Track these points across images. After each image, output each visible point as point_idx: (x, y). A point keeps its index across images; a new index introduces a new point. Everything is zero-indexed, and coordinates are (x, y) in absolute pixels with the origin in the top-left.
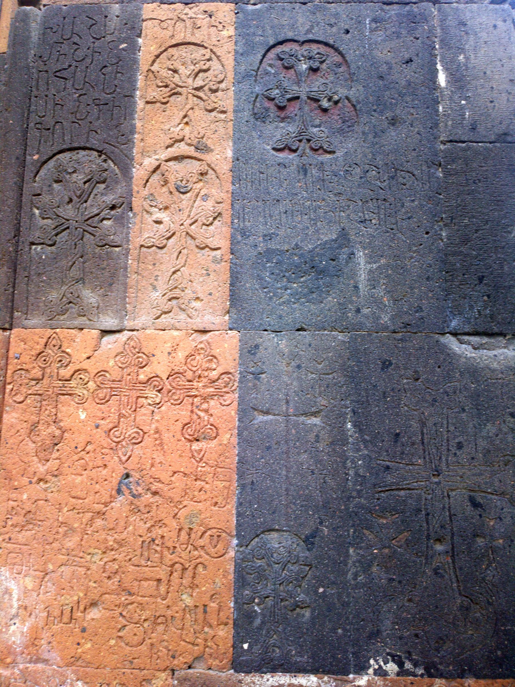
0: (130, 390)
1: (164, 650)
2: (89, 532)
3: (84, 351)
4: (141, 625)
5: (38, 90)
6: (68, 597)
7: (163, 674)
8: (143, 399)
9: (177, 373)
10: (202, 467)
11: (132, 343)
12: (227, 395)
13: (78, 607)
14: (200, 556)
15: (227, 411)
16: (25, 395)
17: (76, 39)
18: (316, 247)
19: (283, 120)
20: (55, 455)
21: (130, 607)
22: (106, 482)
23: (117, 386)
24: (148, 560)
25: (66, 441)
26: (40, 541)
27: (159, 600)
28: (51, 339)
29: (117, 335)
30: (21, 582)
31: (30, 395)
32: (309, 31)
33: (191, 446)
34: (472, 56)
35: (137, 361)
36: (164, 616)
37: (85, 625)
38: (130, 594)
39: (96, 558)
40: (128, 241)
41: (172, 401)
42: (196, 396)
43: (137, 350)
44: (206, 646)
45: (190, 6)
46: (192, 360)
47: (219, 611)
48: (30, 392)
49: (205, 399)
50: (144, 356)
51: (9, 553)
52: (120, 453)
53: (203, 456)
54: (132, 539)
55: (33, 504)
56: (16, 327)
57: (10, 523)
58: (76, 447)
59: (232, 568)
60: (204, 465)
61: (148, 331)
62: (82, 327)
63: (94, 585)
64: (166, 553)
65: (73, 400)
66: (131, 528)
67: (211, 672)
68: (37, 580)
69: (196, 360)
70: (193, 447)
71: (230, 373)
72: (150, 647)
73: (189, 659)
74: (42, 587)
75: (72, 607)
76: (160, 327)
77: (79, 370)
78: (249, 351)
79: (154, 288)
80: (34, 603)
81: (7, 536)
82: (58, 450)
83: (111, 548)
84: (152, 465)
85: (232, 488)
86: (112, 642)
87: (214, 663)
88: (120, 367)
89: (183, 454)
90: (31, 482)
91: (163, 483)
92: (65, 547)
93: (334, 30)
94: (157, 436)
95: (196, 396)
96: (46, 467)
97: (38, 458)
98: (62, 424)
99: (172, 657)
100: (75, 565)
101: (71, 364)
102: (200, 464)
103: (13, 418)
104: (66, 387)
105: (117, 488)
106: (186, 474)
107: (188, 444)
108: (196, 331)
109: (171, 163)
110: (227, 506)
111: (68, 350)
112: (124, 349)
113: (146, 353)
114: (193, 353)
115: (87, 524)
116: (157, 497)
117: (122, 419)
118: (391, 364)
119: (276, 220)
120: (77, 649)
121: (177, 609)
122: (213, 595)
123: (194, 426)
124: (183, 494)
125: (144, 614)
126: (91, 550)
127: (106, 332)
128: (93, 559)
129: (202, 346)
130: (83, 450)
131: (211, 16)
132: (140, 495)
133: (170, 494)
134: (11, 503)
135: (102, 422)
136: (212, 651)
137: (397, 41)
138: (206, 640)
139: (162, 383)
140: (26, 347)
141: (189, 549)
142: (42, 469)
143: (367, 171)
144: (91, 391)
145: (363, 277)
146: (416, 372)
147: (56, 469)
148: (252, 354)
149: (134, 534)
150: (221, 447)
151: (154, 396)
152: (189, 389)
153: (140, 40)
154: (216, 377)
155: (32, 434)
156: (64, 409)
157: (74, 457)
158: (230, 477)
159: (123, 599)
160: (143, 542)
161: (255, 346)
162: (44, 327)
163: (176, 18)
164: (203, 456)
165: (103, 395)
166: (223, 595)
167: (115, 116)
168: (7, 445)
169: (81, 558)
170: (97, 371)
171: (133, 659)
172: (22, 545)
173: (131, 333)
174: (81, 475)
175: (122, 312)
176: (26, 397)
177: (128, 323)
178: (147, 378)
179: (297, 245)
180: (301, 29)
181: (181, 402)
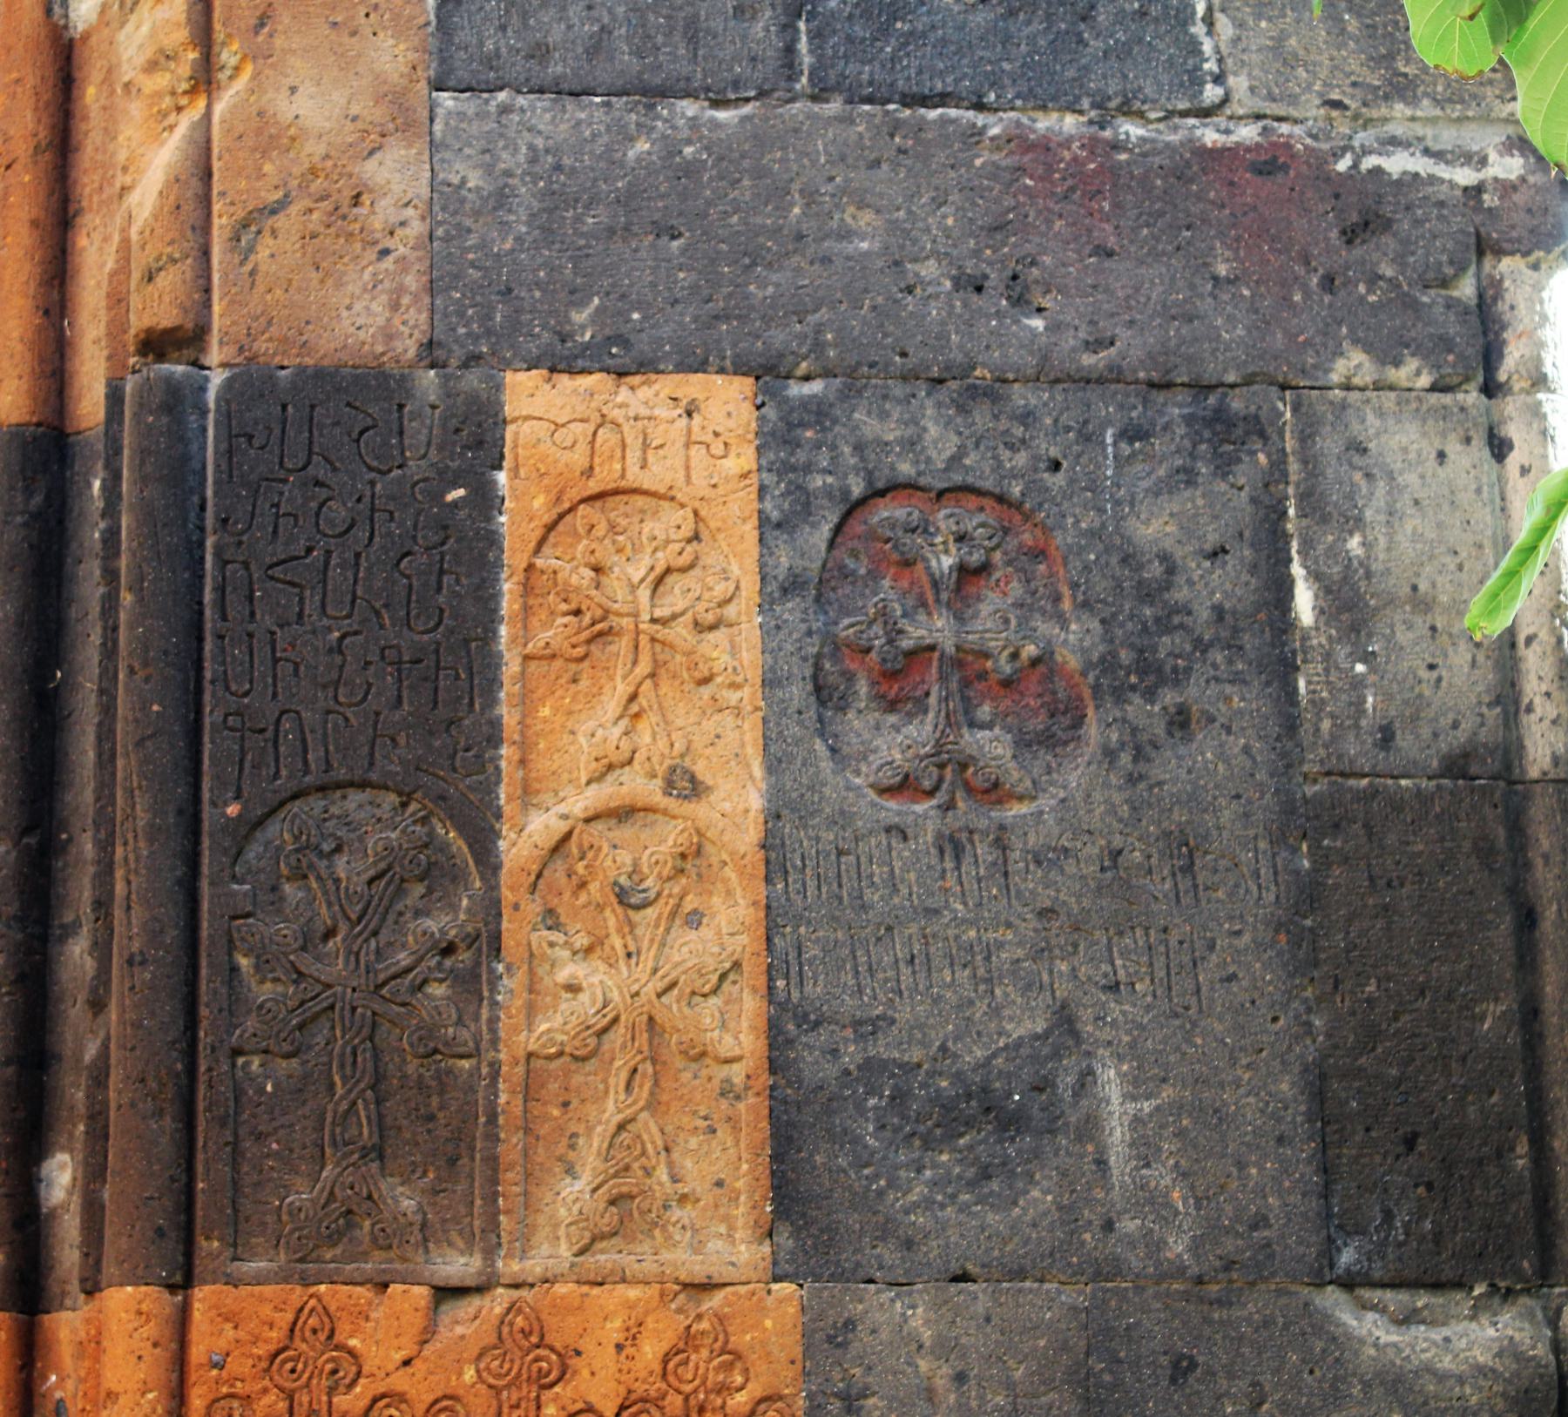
3: (396, 1342)
5: (224, 618)
9: (644, 1400)
11: (520, 1321)
17: (319, 469)
18: (994, 1055)
19: (892, 706)
29: (475, 1302)
32: (955, 460)
34: (1382, 541)
35: (535, 1367)
40: (494, 1042)
43: (534, 1339)
45: (629, 379)
56: (205, 1282)
61: (561, 1289)
62: (387, 1278)
71: (781, 1398)
76: (592, 1277)
77: (383, 1396)
78: (828, 1338)
79: (570, 1171)
88: (490, 1386)
93: (1021, 459)
101: (362, 1381)
108: (686, 1286)
109: (599, 826)
111: (353, 1342)
112: (500, 1337)
113: (558, 1345)
114: (681, 1345)
118: (1193, 1365)
119: (886, 980)
127: (447, 1293)
129: (704, 1325)
131: (689, 414)
137: (1187, 494)
140: (241, 1334)
143: (1120, 852)
145: (1117, 1135)
146: (1254, 1384)
148: (839, 1345)
153: (502, 477)
161: (845, 1325)
162: (286, 1281)
163: (596, 418)
167: (441, 695)
170: (430, 1398)
173: (515, 1294)
175: (488, 1240)
177: (509, 1267)
179: (943, 1048)
180: (934, 455)
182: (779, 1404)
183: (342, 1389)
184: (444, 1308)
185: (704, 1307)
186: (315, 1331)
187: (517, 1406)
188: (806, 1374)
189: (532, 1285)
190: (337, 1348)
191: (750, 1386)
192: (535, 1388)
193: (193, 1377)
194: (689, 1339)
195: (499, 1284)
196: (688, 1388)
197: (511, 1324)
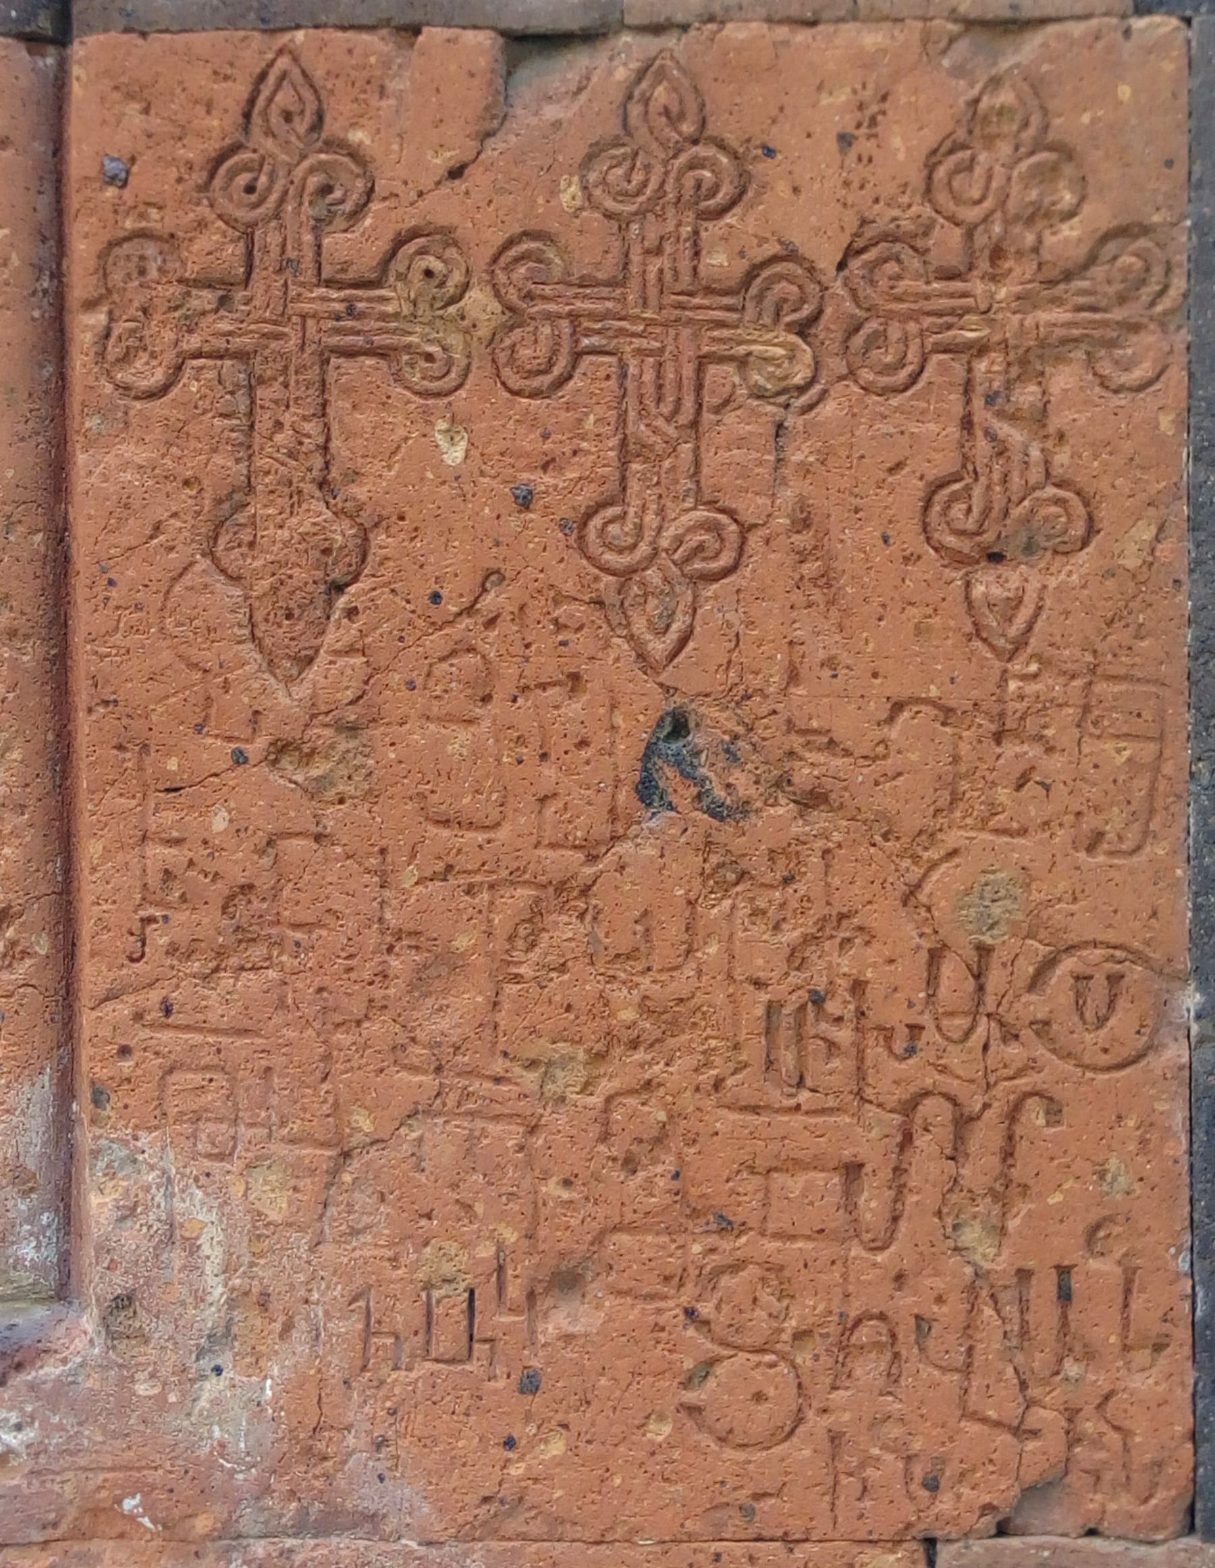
0: (665, 325)
1: (889, 1457)
2: (522, 970)
4: (783, 1357)
6: (452, 1248)
7: (892, 1558)
8: (729, 368)
9: (886, 237)
10: (1024, 677)
11: (661, 94)
12: (1134, 338)
13: (501, 1288)
14: (1031, 1066)
15: (1137, 417)
16: (169, 357)
20: (337, 635)
21: (726, 1281)
22: (584, 754)
23: (599, 307)
24: (801, 1083)
25: (388, 572)
26: (308, 1011)
27: (856, 1251)
28: (271, 79)
29: (579, 61)
30: (237, 1190)
31: (198, 355)
33: (968, 585)
35: (689, 180)
36: (882, 1317)
37: (534, 1363)
38: (726, 1227)
39: (566, 1081)
41: (867, 375)
42: (981, 349)
43: (687, 128)
44: (1073, 1439)
46: (957, 171)
47: (1128, 1291)
48: (193, 342)
49: (1029, 361)
50: (724, 160)
51: (171, 1071)
52: (639, 625)
53: (1029, 628)
54: (720, 998)
55: (262, 853)
56: (90, 29)
57: (159, 939)
58: (436, 598)
59: (1179, 1118)
60: (1033, 667)
61: (735, 32)
63: (566, 1195)
64: (875, 1051)
65: (398, 378)
66: (713, 949)
67: (1097, 1543)
68: (306, 1183)
69: (978, 171)
70: (978, 590)
71: (1146, 230)
72: (826, 1445)
73: (1000, 1491)
74: (332, 1211)
75: (472, 1292)
76: (794, 10)
77: (414, 234)
80: (302, 1277)
81: (154, 996)
82: (351, 613)
83: (626, 1035)
84: (793, 676)
85: (1168, 768)
86: (661, 1432)
87: (1112, 1507)
88: (609, 215)
89: (936, 621)
90: (240, 758)
91: (847, 753)
92: (421, 1035)
94: (803, 540)
95: (981, 349)
96: (301, 691)
97: (261, 647)
98: (360, 492)
99: (925, 1485)
100: (472, 1114)
101: (375, 206)
102: (1016, 667)
103: (125, 465)
104: (361, 316)
105: (637, 777)
106: (949, 711)
107: (957, 576)
108: (971, 24)
110: (1148, 849)
111: (357, 136)
113: (732, 139)
114: (961, 135)
115: (511, 938)
116: (820, 819)
117: (635, 466)
120: (507, 1463)
121: (939, 1284)
122: (1097, 1227)
123: (977, 491)
124: (944, 798)
125: (794, 1312)
126: (540, 1048)
127: (528, 44)
128: (550, 1087)
129: (1006, 97)
130: (470, 610)
132: (744, 808)
133: (884, 800)
134: (157, 852)
135: (548, 479)
136: (1102, 1455)
138: (1071, 1414)
139: (812, 288)
141: (981, 1030)
142: (286, 700)
144: (484, 332)
147: (350, 695)
149: (730, 977)
150: (1110, 583)
151: (780, 351)
152: (952, 312)
154: (1083, 251)
155: (222, 541)
156: (364, 419)
157: (427, 641)
158: (1161, 717)
159: (696, 1248)
160: (772, 1009)
162: (232, 23)
164: (1029, 628)
165: (542, 351)
166: (1143, 1224)
168: (114, 593)
169: (498, 1080)
170: (500, 238)
171: (758, 1497)
172: (225, 1032)
173: (652, 44)
174: (470, 722)
176: (179, 368)
178: (742, 266)
181: (914, 378)
182: (1143, 243)
183: (340, 223)
184: (523, 73)
185: (1004, 65)
186: (288, 117)
187: (659, 251)
188: (1195, 185)
189: (685, 28)
190: (330, 145)
191: (1087, 209)
192: (690, 216)
193: (74, 201)
194: (976, 123)
195: (623, 27)
196: (972, 214)
197: (646, 101)
